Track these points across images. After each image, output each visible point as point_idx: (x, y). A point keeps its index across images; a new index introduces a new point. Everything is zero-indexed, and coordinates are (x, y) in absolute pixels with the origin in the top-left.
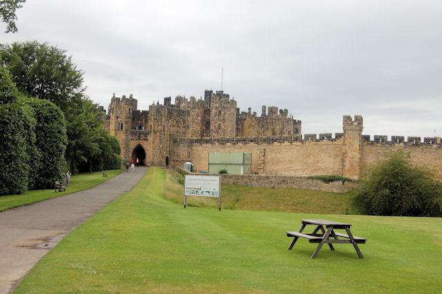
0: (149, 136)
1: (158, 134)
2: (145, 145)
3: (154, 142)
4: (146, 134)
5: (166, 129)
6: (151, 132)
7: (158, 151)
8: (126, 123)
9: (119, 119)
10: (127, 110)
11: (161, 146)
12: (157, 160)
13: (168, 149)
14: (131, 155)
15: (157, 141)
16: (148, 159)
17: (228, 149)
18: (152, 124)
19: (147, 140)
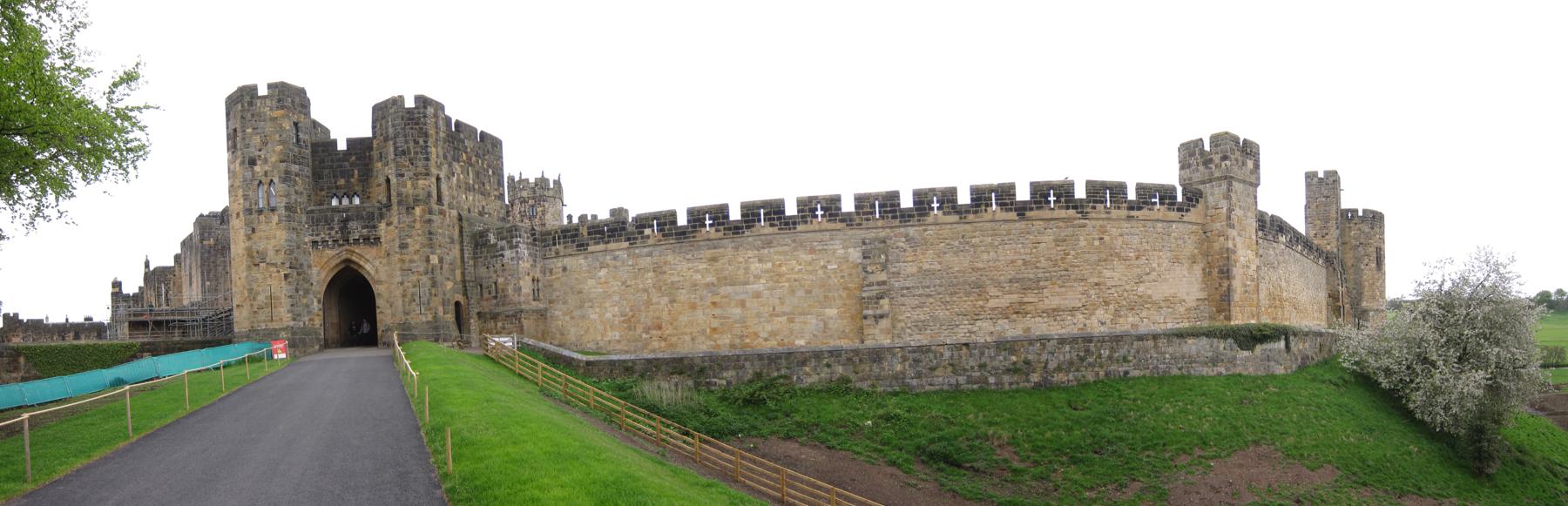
0: (382, 226)
1: (418, 211)
2: (373, 265)
3: (403, 246)
4: (371, 219)
5: (444, 187)
6: (388, 206)
7: (425, 279)
8: (287, 178)
9: (257, 168)
10: (287, 125)
11: (434, 260)
12: (421, 317)
13: (458, 272)
14: (316, 306)
15: (414, 244)
16: (387, 313)
17: (709, 253)
18: (391, 171)
19: (378, 239)
